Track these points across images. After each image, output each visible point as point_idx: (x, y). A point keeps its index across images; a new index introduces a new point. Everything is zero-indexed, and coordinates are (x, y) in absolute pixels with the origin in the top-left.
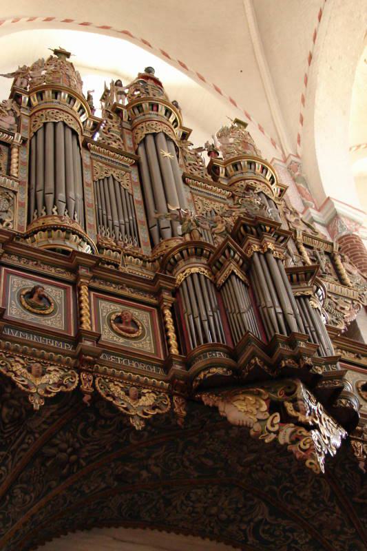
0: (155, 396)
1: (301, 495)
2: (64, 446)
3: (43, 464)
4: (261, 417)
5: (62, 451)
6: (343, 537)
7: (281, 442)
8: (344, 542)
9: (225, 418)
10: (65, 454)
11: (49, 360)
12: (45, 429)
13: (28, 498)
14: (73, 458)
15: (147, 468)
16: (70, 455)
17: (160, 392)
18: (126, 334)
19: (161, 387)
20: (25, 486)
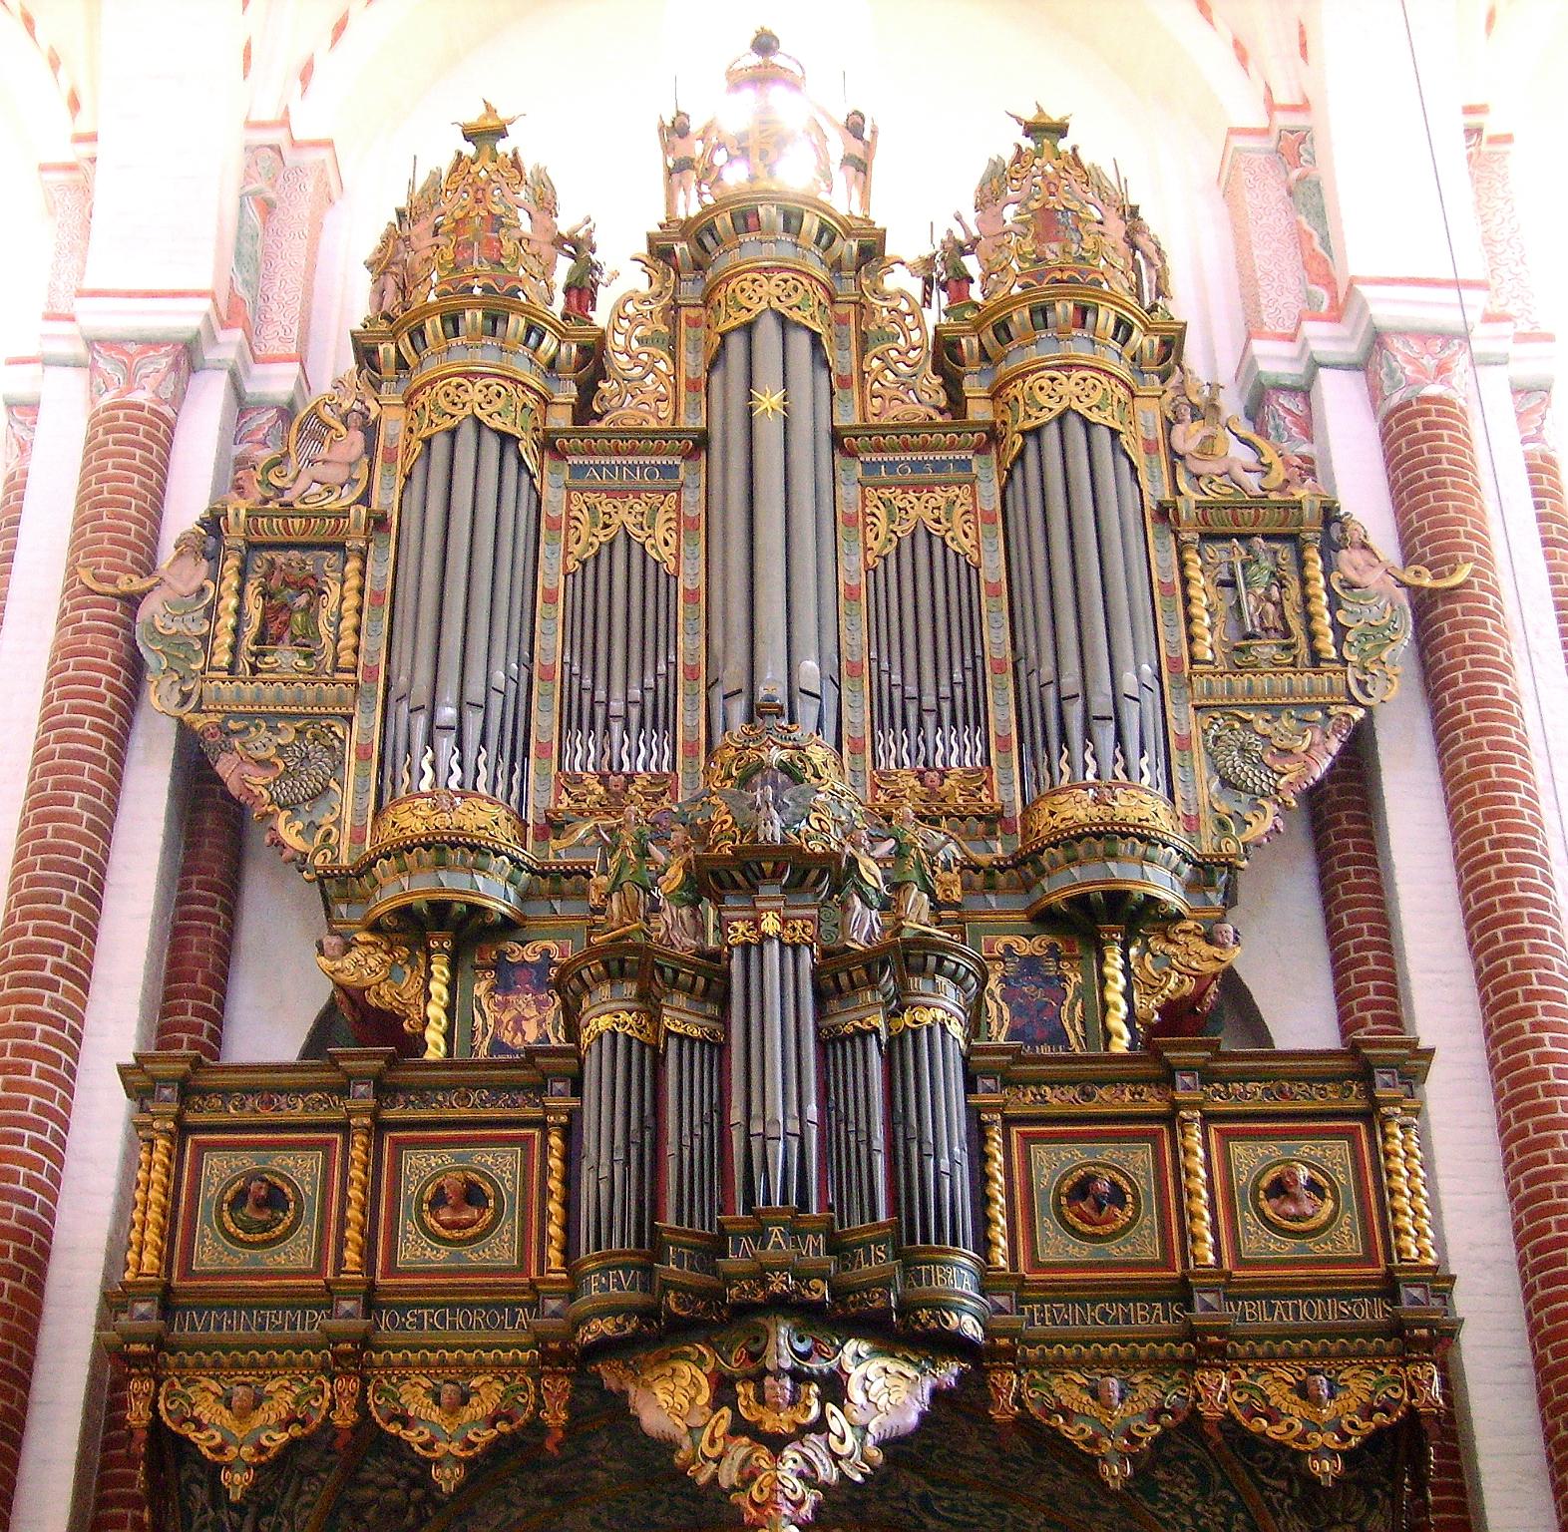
0: (502, 1388)
1: (969, 1451)
3: (357, 1518)
4: (697, 1421)
5: (384, 1488)
6: (1104, 1517)
7: (724, 1482)
9: (637, 1419)
10: (395, 1491)
11: (268, 1367)
14: (417, 1494)
15: (595, 1465)
17: (513, 1376)
18: (460, 1236)
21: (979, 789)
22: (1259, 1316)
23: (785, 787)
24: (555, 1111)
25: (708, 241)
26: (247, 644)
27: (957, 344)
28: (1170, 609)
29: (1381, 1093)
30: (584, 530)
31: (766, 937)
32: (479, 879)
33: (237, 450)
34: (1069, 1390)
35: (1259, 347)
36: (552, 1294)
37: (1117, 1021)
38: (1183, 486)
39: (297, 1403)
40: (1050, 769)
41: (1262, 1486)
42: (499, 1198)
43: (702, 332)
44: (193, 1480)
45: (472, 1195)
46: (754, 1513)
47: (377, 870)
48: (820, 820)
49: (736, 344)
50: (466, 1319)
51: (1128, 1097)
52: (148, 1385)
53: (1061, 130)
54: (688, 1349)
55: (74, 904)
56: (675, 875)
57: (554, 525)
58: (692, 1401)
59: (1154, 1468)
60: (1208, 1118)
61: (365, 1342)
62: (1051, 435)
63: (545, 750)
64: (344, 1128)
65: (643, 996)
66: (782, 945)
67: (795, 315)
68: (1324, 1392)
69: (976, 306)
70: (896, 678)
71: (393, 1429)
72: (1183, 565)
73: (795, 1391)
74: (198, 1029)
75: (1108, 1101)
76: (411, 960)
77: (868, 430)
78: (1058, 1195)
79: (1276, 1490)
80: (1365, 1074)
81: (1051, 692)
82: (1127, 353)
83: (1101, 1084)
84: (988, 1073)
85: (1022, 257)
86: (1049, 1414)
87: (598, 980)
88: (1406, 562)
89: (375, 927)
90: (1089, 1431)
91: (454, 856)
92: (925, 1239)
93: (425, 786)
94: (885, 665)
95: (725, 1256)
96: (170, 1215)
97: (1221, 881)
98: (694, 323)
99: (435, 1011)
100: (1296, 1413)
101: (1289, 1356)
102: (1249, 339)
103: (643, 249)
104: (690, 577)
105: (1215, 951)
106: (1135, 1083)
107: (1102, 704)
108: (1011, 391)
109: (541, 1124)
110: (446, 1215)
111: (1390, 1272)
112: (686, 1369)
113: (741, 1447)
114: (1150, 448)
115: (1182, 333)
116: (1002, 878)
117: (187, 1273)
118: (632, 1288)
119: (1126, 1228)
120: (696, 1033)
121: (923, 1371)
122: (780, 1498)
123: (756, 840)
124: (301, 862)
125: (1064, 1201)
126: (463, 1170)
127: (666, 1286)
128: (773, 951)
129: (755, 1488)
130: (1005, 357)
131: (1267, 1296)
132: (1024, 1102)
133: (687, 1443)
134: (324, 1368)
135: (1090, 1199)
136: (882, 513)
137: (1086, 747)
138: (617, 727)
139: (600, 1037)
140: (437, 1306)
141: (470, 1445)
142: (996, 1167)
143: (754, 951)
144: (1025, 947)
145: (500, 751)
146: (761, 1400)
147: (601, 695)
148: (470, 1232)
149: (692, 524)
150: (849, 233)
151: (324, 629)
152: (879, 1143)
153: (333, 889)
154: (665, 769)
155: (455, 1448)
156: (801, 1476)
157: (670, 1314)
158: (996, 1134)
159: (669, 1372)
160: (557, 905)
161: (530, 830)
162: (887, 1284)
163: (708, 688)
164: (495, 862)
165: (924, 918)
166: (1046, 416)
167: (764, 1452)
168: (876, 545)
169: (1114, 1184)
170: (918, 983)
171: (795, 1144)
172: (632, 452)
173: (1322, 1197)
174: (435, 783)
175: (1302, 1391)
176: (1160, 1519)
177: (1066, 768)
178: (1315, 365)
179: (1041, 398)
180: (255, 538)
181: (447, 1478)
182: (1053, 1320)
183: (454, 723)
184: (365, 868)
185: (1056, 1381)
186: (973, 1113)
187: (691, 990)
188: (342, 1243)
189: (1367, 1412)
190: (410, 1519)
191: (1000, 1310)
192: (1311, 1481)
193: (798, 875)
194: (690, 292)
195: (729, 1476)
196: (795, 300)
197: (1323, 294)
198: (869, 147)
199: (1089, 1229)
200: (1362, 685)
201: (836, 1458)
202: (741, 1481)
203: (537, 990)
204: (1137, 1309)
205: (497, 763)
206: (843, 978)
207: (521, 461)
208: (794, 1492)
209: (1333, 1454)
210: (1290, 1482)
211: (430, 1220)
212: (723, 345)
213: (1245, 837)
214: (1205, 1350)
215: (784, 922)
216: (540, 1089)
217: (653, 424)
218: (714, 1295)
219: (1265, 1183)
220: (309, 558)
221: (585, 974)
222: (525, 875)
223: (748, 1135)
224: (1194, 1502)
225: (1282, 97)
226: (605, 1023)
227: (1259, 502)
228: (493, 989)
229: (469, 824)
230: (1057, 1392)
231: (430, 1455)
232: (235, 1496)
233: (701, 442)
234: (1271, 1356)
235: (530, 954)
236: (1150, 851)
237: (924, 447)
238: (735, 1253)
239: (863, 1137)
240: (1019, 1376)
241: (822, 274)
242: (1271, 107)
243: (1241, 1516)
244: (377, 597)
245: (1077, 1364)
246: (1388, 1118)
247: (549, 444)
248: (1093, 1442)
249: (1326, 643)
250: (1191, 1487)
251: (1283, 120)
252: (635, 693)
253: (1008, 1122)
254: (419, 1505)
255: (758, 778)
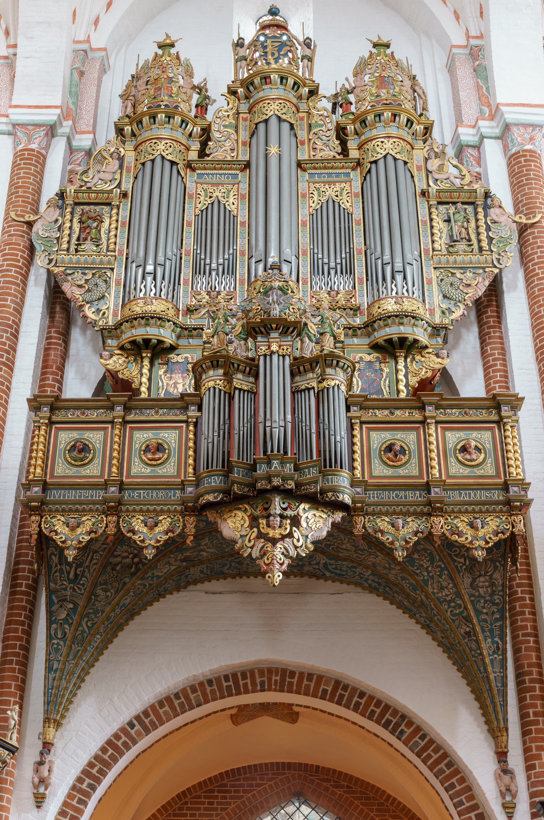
1: (344, 547)
2: (125, 554)
3: (113, 569)
4: (244, 533)
6: (393, 572)
7: (254, 556)
8: (396, 575)
9: (221, 533)
12: (105, 548)
13: (109, 594)
14: (136, 560)
15: (203, 550)
16: (133, 559)
17: (174, 516)
18: (153, 463)
19: (175, 511)
20: (104, 587)
21: (351, 298)
22: (455, 496)
23: (281, 296)
24: (192, 417)
25: (251, 88)
26: (74, 241)
27: (345, 128)
28: (425, 231)
29: (503, 414)
30: (202, 198)
31: (272, 353)
32: (162, 331)
33: (69, 167)
34: (383, 523)
35: (461, 130)
36: (190, 485)
37: (402, 387)
38: (431, 183)
39: (93, 525)
40: (378, 290)
41: (454, 561)
42: (169, 449)
43: (248, 123)
44: (53, 554)
45: (159, 448)
46: (265, 568)
47: (123, 327)
48: (293, 308)
49: (262, 127)
50: (157, 494)
51: (407, 414)
52: (38, 518)
53: (388, 46)
54: (241, 506)
55: (7, 338)
56: (239, 329)
57: (191, 197)
58: (242, 525)
59: (414, 554)
60: (437, 423)
61: (120, 503)
62: (381, 163)
63: (186, 282)
64: (112, 422)
65: (225, 374)
66: (279, 355)
67: (284, 117)
68: (480, 526)
69: (353, 113)
70: (320, 256)
71: (129, 535)
72: (430, 214)
73: (281, 522)
74: (54, 386)
75: (399, 414)
76: (135, 360)
77: (311, 161)
78: (380, 451)
79: (459, 563)
80: (498, 408)
81: (380, 261)
82: (411, 131)
83: (397, 409)
84: (355, 405)
85: (372, 95)
86: (376, 532)
87: (208, 368)
88: (516, 214)
89: (122, 348)
90: (391, 539)
91: (152, 321)
92: (331, 466)
93: (142, 295)
94: (316, 251)
95: (256, 471)
96: (46, 453)
97: (443, 333)
98: (245, 120)
99: (144, 380)
100: (469, 533)
101: (467, 512)
102: (457, 127)
103: (225, 90)
104: (243, 216)
105: (439, 360)
106: (410, 409)
107: (398, 266)
108: (366, 146)
109: (186, 422)
110: (150, 456)
111: (506, 481)
112: (240, 514)
113: (260, 543)
114: (419, 168)
115: (432, 125)
116: (359, 332)
117: (52, 476)
118: (221, 483)
119: (406, 463)
120: (246, 388)
121: (329, 516)
122: (275, 562)
123: (270, 316)
124: (94, 324)
125: (382, 453)
126: (156, 439)
127: (233, 482)
128: (275, 357)
129: (265, 559)
130: (363, 134)
131: (459, 490)
132: (368, 416)
133: (240, 541)
134: (104, 513)
135: (392, 452)
136: (316, 193)
137: (392, 282)
138: (214, 273)
139: (209, 389)
140: (146, 489)
141: (158, 541)
142: (357, 440)
143: (268, 357)
144: (368, 358)
145: (170, 282)
146: (268, 525)
147: (208, 261)
148: (159, 462)
149: (243, 197)
150: (305, 85)
151: (104, 236)
152: (314, 430)
153: (106, 333)
154: (232, 290)
155: (152, 542)
156: (283, 554)
157: (235, 493)
158: (357, 427)
159: (233, 515)
160: (191, 340)
161: (181, 312)
162: (316, 482)
163: (249, 259)
164: (168, 324)
165: (332, 346)
166: (380, 156)
167: (270, 545)
168: (313, 205)
169: (401, 447)
170: (329, 371)
171: (282, 429)
172: (221, 169)
173: (480, 453)
174: (145, 294)
175: (472, 525)
176: (415, 573)
177: (385, 291)
178: (482, 138)
179: (378, 149)
180: (77, 201)
181: (149, 553)
182: (377, 497)
183: (153, 272)
184: (118, 326)
185: (378, 520)
186: (350, 419)
187: (244, 372)
188: (111, 466)
189: (496, 533)
190: (133, 570)
191: (358, 493)
192: (474, 559)
193: (285, 329)
194: (244, 107)
195: (255, 553)
196: (284, 111)
197: (486, 110)
198: (314, 51)
199: (391, 463)
200: (498, 260)
201: (296, 547)
202: (261, 556)
203: (183, 373)
204: (410, 494)
205: (169, 287)
206: (302, 368)
207: (179, 172)
208: (280, 559)
209: (483, 549)
210: (465, 560)
211: (144, 458)
212: (256, 128)
213: (451, 318)
214: (434, 509)
215: (280, 346)
216: (185, 409)
217: (229, 158)
218: (252, 486)
219: (459, 447)
220: (98, 208)
221: (204, 366)
222: (179, 330)
223: (265, 427)
224: (428, 567)
225: (473, 33)
226: (211, 384)
227: (460, 189)
228: (166, 372)
229: (158, 310)
230: (379, 524)
231: (143, 545)
232: (70, 559)
233: (248, 165)
234: (460, 512)
235: (180, 359)
236: (416, 322)
237: (332, 168)
238: (260, 470)
239: (308, 428)
240: (365, 518)
241: (294, 100)
242: (468, 37)
243: (446, 572)
244: (123, 224)
245: (387, 514)
246: (505, 424)
247: (189, 166)
248: (392, 543)
249: (485, 244)
250: (428, 561)
251: (473, 42)
252: (221, 261)
253: (362, 423)
254: (137, 564)
255: (270, 293)
